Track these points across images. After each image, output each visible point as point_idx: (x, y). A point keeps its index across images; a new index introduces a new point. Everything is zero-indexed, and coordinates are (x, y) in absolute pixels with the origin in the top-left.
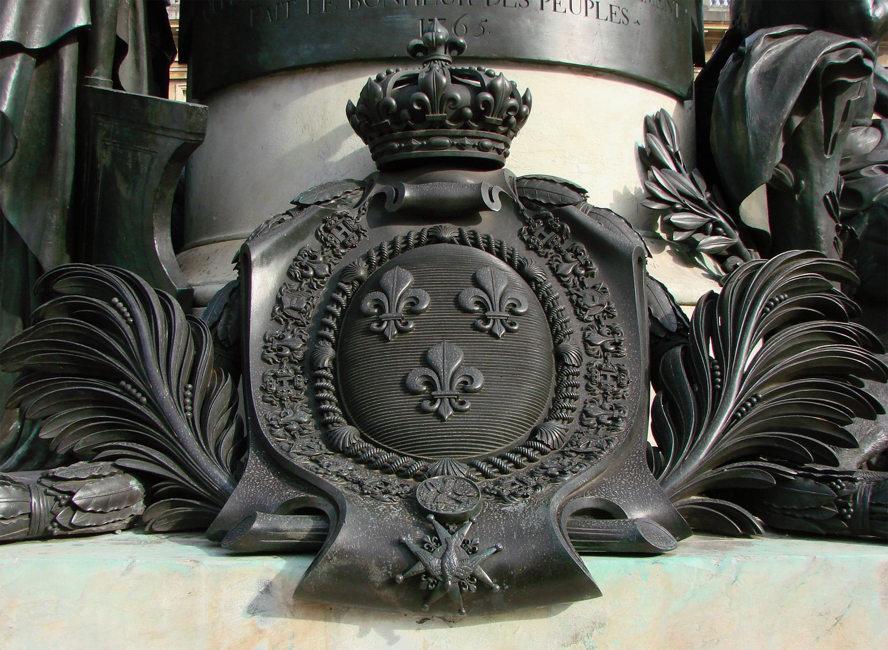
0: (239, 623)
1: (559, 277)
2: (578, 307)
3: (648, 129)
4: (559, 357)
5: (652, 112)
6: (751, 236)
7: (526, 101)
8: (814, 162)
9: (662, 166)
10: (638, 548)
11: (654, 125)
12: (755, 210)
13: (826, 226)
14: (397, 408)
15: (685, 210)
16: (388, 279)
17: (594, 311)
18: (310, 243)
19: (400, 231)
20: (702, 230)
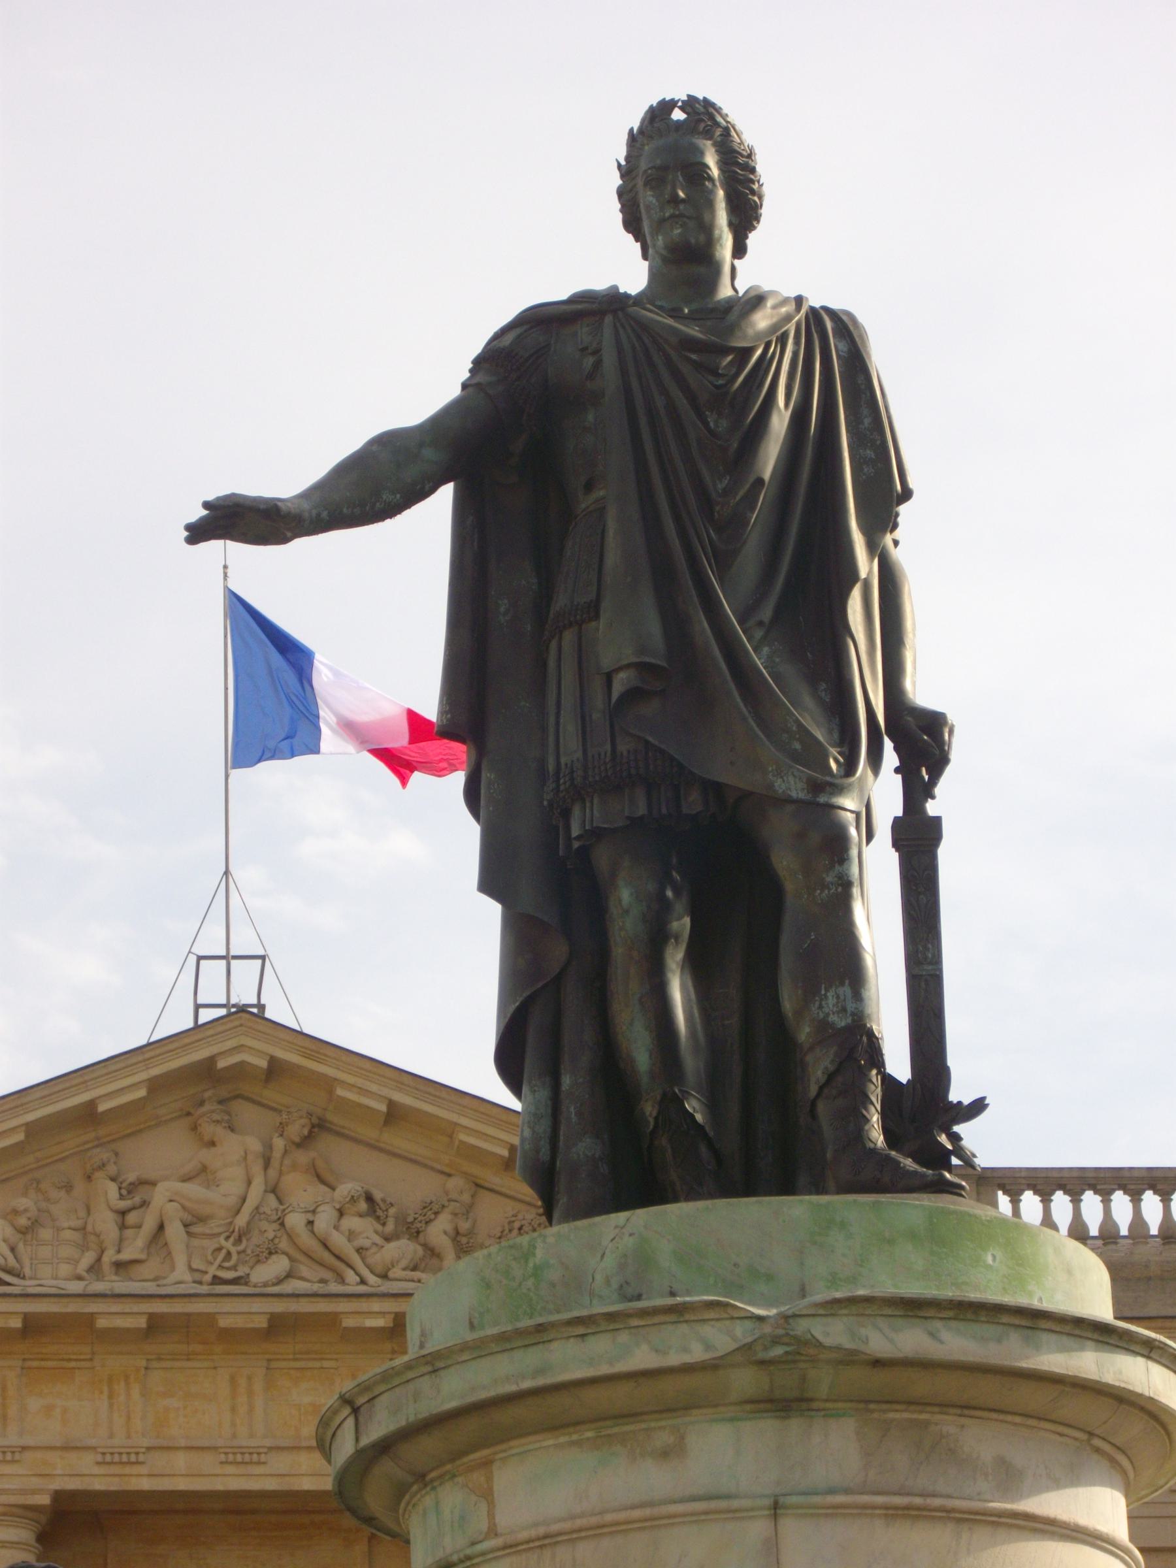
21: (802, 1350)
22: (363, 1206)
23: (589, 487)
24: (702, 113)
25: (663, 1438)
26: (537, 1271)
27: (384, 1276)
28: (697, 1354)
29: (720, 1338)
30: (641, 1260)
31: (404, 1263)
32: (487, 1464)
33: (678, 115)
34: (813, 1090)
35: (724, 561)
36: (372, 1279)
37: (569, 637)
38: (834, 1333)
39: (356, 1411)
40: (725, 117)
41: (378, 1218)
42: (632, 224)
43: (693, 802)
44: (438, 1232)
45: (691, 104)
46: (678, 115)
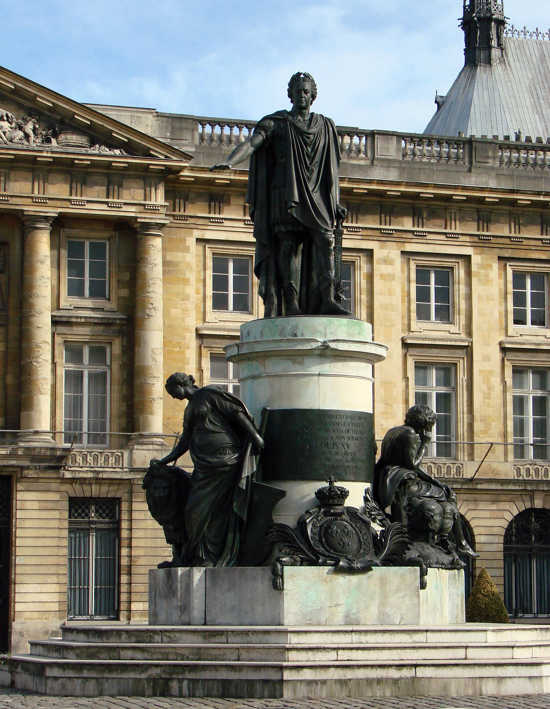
0: (326, 575)
1: (357, 527)
2: (361, 532)
3: (366, 493)
4: (360, 540)
5: (366, 488)
6: (387, 515)
7: (348, 492)
8: (401, 498)
9: (369, 501)
10: (377, 565)
11: (367, 491)
12: (388, 510)
13: (404, 513)
14: (339, 547)
15: (374, 511)
16: (332, 526)
17: (363, 532)
18: (315, 520)
19: (330, 518)
20: (378, 515)
21: (328, 347)
22: (5, 118)
23: (282, 158)
24: (307, 76)
25: (299, 360)
26: (276, 326)
27: (11, 141)
28: (309, 348)
29: (314, 345)
30: (296, 327)
31: (18, 138)
32: (264, 360)
33: (302, 76)
34: (322, 290)
35: (309, 179)
36: (8, 142)
37: (277, 191)
38: (333, 345)
39: (238, 347)
40: (312, 77)
41: (9, 122)
42: (290, 96)
43: (301, 229)
44: (29, 128)
45: (304, 75)
46: (302, 76)
